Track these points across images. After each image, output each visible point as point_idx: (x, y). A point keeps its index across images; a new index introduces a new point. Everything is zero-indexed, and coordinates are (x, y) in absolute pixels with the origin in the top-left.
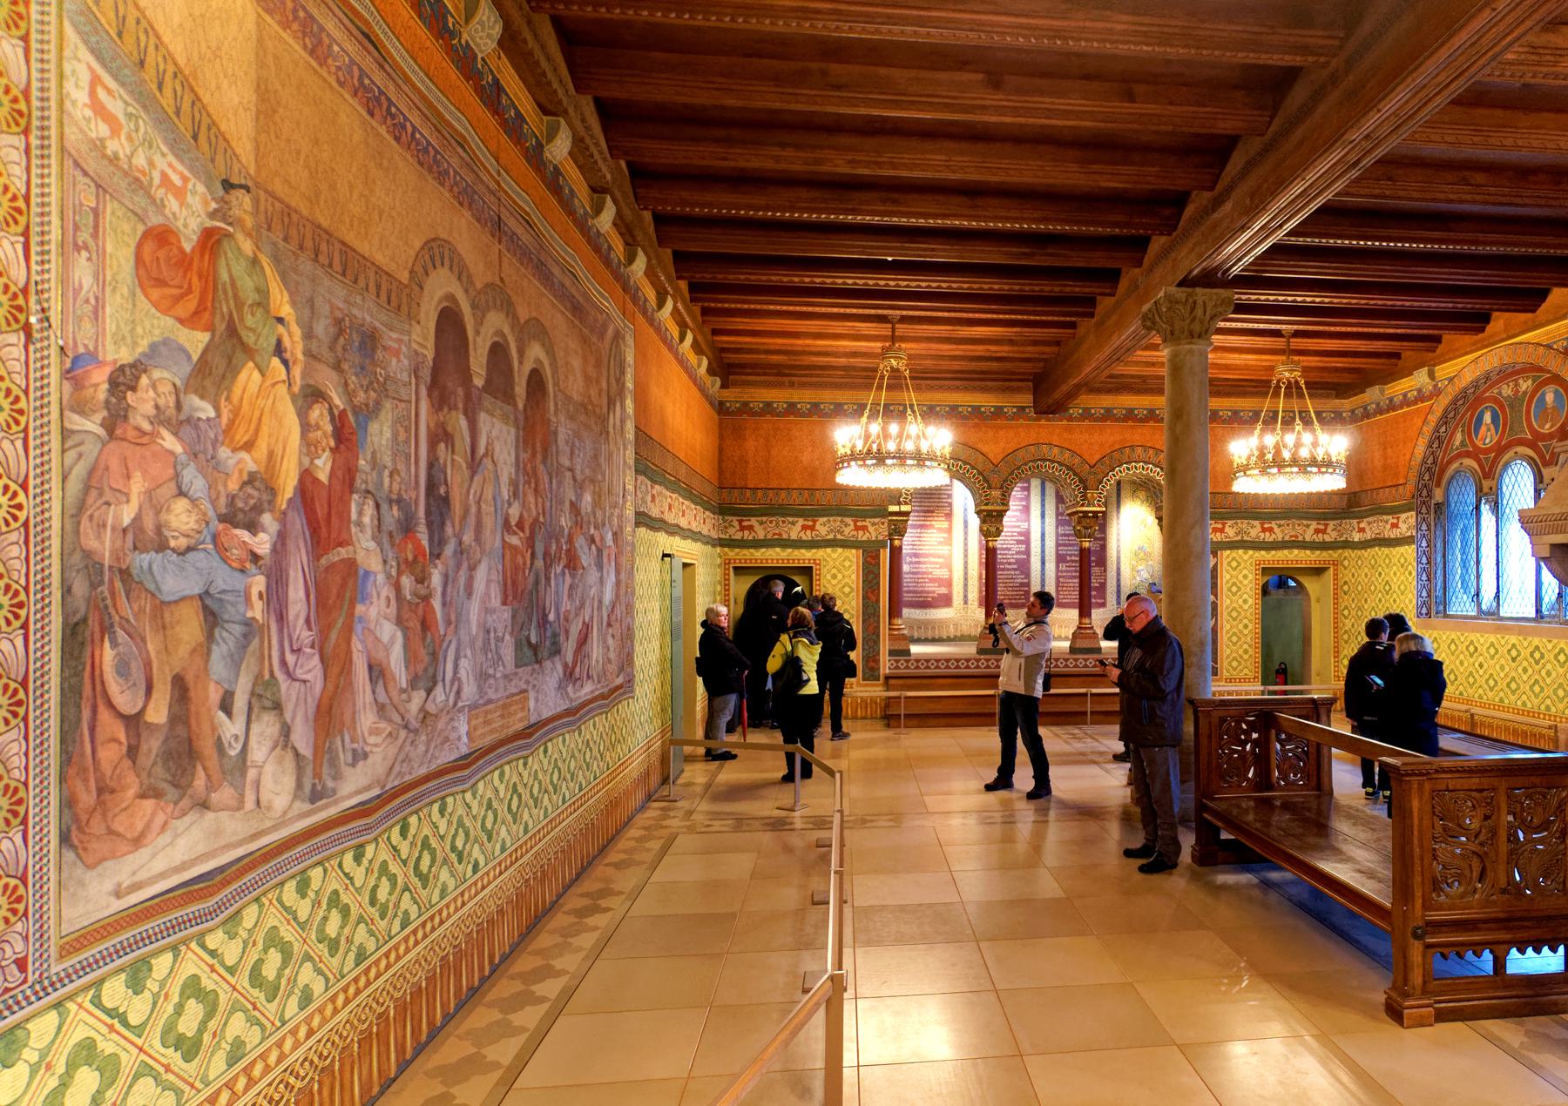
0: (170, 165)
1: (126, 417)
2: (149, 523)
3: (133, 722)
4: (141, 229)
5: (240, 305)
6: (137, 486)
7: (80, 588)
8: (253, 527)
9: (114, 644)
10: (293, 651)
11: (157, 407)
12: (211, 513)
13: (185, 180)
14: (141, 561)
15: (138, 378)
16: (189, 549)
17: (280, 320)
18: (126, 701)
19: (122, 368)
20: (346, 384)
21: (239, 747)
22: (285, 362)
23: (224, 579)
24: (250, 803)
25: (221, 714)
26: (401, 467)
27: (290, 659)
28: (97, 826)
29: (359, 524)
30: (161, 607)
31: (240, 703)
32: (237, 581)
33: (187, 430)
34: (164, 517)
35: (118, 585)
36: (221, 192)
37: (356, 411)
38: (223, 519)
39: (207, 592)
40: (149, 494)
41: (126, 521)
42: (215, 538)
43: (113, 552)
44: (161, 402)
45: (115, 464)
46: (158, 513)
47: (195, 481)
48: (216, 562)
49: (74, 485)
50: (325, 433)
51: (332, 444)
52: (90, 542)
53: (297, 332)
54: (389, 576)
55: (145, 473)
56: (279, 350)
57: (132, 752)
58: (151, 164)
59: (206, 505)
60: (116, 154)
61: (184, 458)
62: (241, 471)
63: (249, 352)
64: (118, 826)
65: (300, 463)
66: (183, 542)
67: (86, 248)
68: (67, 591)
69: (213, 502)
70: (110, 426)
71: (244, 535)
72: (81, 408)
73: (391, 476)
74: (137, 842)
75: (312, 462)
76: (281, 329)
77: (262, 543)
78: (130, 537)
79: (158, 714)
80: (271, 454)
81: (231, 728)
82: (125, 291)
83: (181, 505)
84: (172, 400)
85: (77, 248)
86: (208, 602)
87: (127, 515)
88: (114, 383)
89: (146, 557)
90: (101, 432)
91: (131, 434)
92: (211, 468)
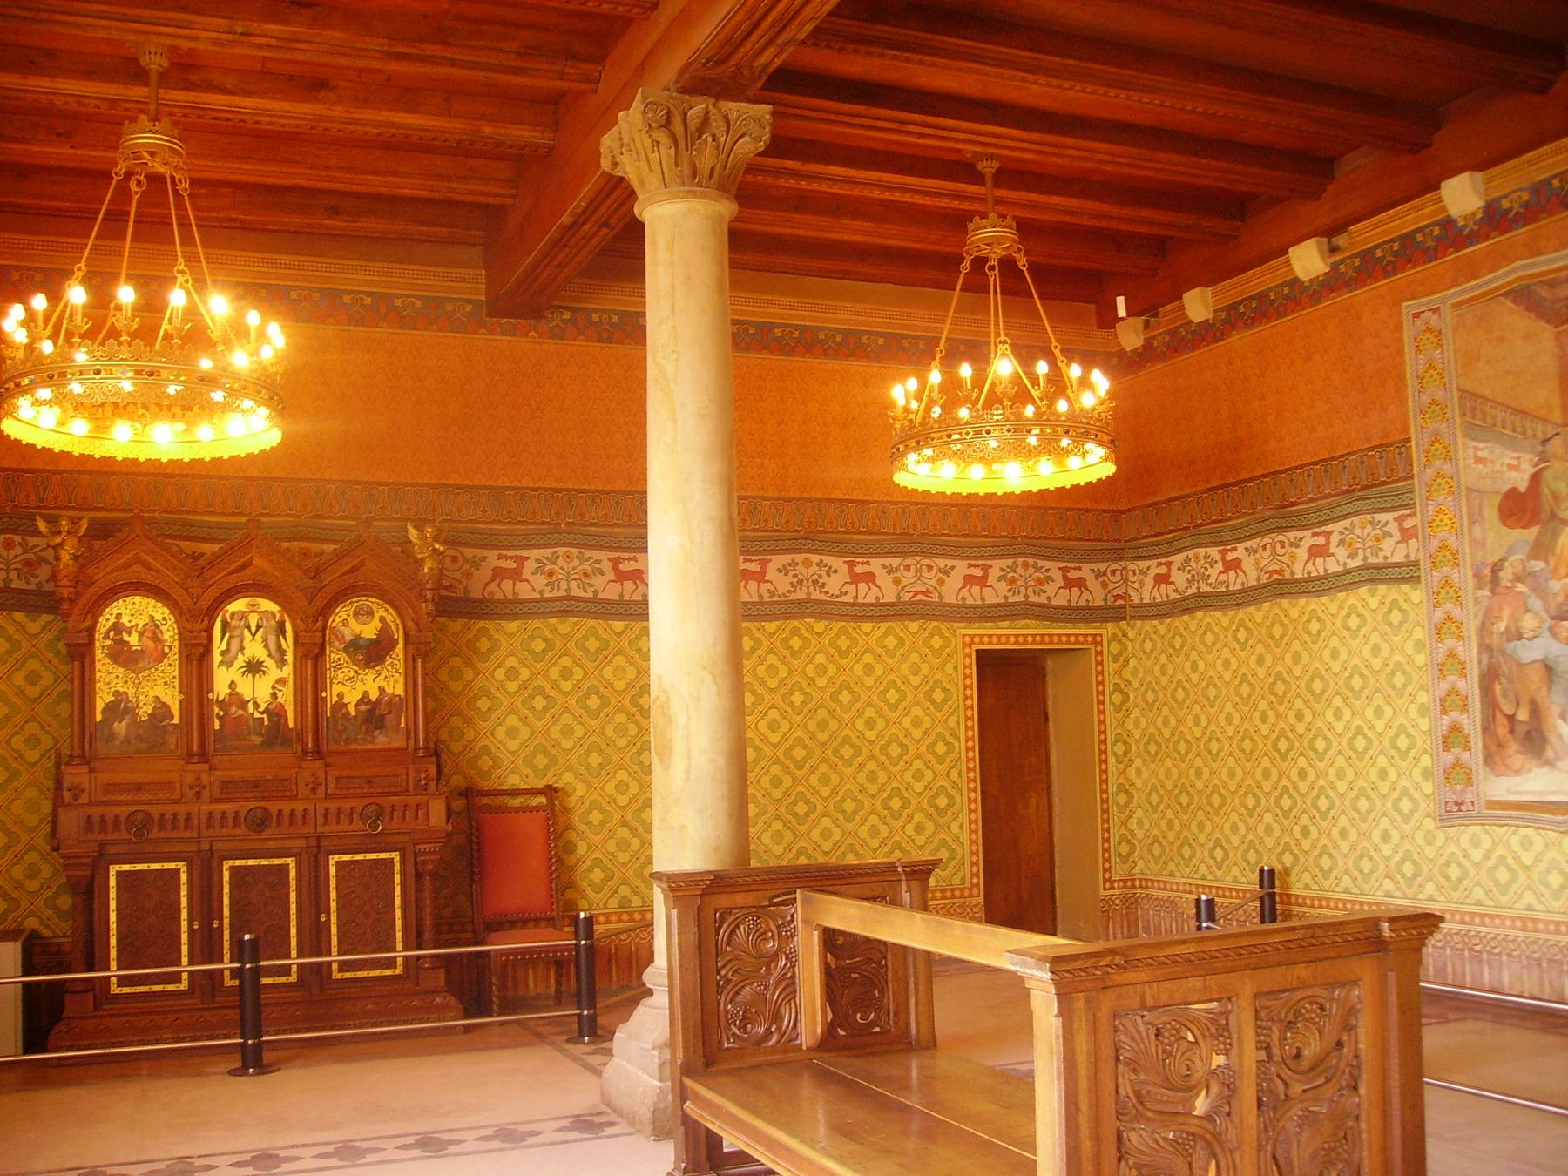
3: (1511, 718)
5: (1556, 497)
6: (1506, 613)
12: (1545, 616)
18: (1507, 708)
28: (1497, 759)
36: (1540, 448)
38: (1553, 618)
42: (1551, 630)
47: (1536, 603)
49: (1480, 618)
52: (1487, 641)
57: (1512, 732)
59: (1543, 614)
66: (1531, 634)
70: (1492, 591)
72: (1479, 587)
74: (1517, 773)
79: (1523, 715)
83: (1528, 616)
87: (1502, 629)
88: (1493, 571)
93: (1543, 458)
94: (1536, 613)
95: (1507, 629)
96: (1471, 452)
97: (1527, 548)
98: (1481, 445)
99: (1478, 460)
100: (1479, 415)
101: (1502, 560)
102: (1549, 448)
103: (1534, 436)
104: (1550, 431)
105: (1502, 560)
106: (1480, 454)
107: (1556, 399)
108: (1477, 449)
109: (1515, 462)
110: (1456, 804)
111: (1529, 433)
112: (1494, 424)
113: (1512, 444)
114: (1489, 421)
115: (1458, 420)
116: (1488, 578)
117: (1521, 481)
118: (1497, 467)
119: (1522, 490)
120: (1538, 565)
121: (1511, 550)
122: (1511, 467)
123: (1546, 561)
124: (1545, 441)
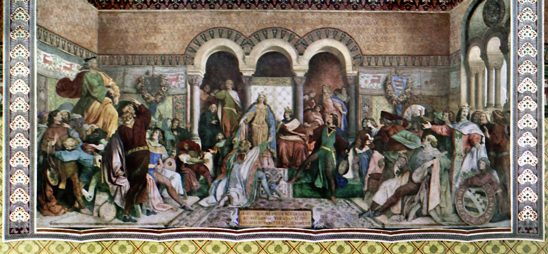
0: (67, 64)
1: (53, 123)
2: (60, 144)
4: (58, 81)
5: (91, 87)
6: (56, 137)
7: (42, 158)
8: (97, 144)
9: (50, 170)
10: (114, 176)
11: (62, 118)
12: (80, 141)
13: (71, 65)
14: (57, 153)
15: (56, 113)
16: (72, 150)
17: (109, 87)
19: (52, 112)
20: (143, 96)
21: (91, 199)
22: (112, 98)
23: (84, 156)
24: (96, 214)
25: (84, 191)
26: (180, 117)
27: (114, 179)
28: (45, 207)
29: (151, 139)
30: (63, 162)
31: (92, 188)
32: (90, 157)
33: (72, 122)
34: (64, 142)
35: (51, 159)
36: (84, 62)
37: (150, 103)
38: (84, 142)
39: (79, 160)
40: (60, 138)
41: (53, 144)
43: (50, 151)
44: (64, 117)
45: (50, 132)
46: (62, 141)
47: (76, 135)
48: (82, 152)
50: (131, 114)
51: (135, 116)
53: (117, 88)
54: (170, 155)
55: (59, 133)
56: (109, 95)
58: (61, 66)
60: (51, 69)
61: (71, 128)
62: (92, 129)
63: (95, 99)
64: (52, 209)
65: (118, 123)
66: (70, 148)
67: (43, 90)
68: (38, 159)
69: (81, 138)
71: (94, 145)
73: (173, 121)
74: (56, 214)
75: (124, 123)
76: (109, 89)
77: (101, 147)
78: (54, 148)
79: (62, 186)
80: (104, 124)
81: (88, 194)
82: (53, 96)
84: (67, 116)
85: (40, 91)
86: (80, 162)
87: (53, 143)
89: (59, 152)
90: (46, 126)
91: (55, 126)
92: (79, 129)
93: (85, 67)
94: (74, 138)
95: (56, 145)
96: (42, 57)
97: (72, 108)
98: (48, 54)
99: (45, 61)
100: (48, 40)
101: (57, 111)
102: (89, 63)
103: (81, 56)
104: (90, 56)
105: (57, 111)
106: (47, 58)
107: (96, 41)
108: (45, 56)
109: (69, 66)
110: (17, 229)
111: (78, 54)
112: (58, 46)
113: (67, 57)
114: (55, 44)
115: (36, 40)
116: (47, 119)
117: (72, 75)
118: (58, 66)
119: (72, 80)
120: (78, 116)
121: (62, 107)
122: (65, 68)
123: (83, 115)
124: (87, 60)
